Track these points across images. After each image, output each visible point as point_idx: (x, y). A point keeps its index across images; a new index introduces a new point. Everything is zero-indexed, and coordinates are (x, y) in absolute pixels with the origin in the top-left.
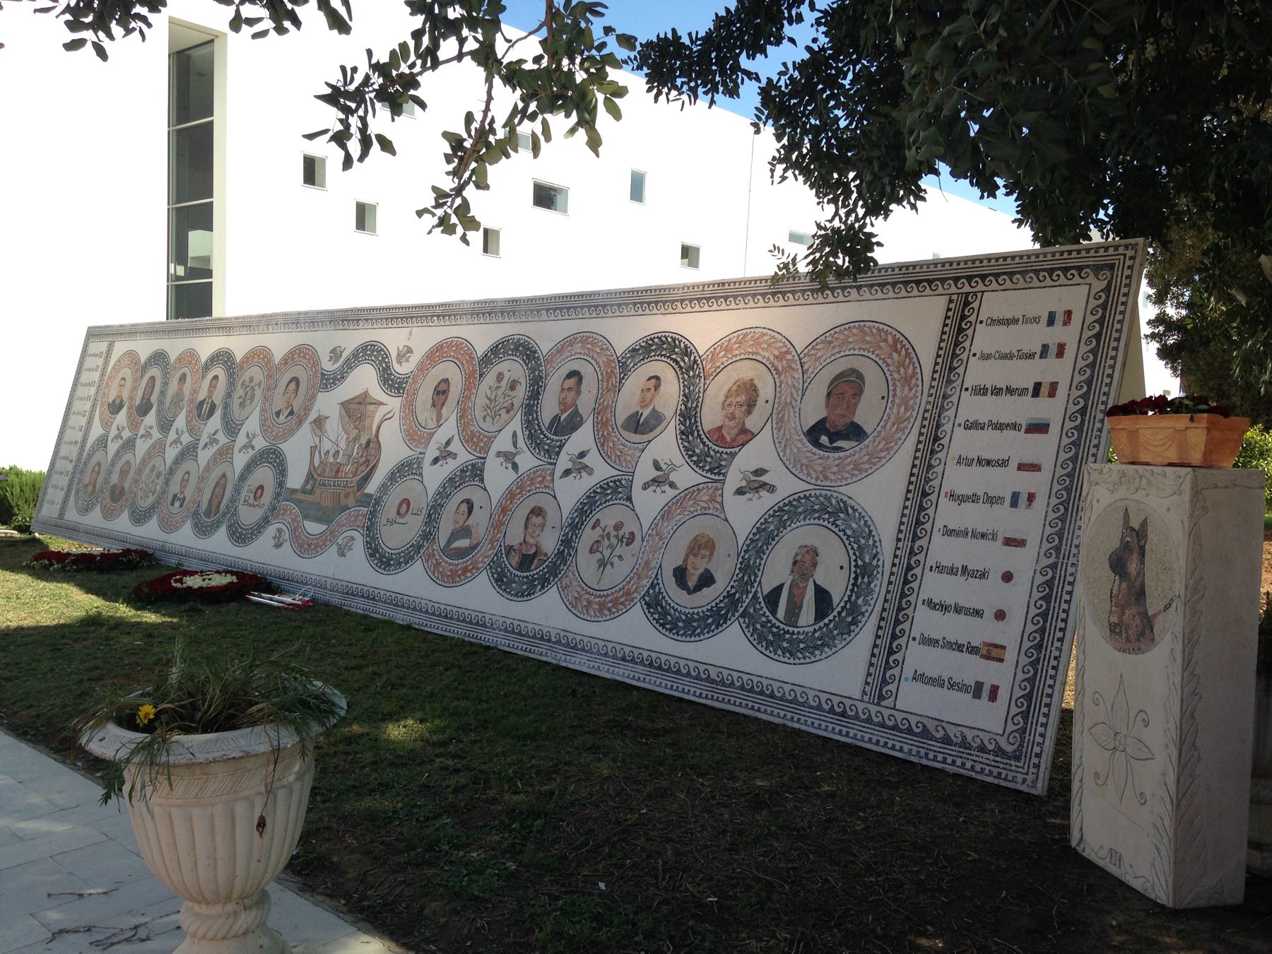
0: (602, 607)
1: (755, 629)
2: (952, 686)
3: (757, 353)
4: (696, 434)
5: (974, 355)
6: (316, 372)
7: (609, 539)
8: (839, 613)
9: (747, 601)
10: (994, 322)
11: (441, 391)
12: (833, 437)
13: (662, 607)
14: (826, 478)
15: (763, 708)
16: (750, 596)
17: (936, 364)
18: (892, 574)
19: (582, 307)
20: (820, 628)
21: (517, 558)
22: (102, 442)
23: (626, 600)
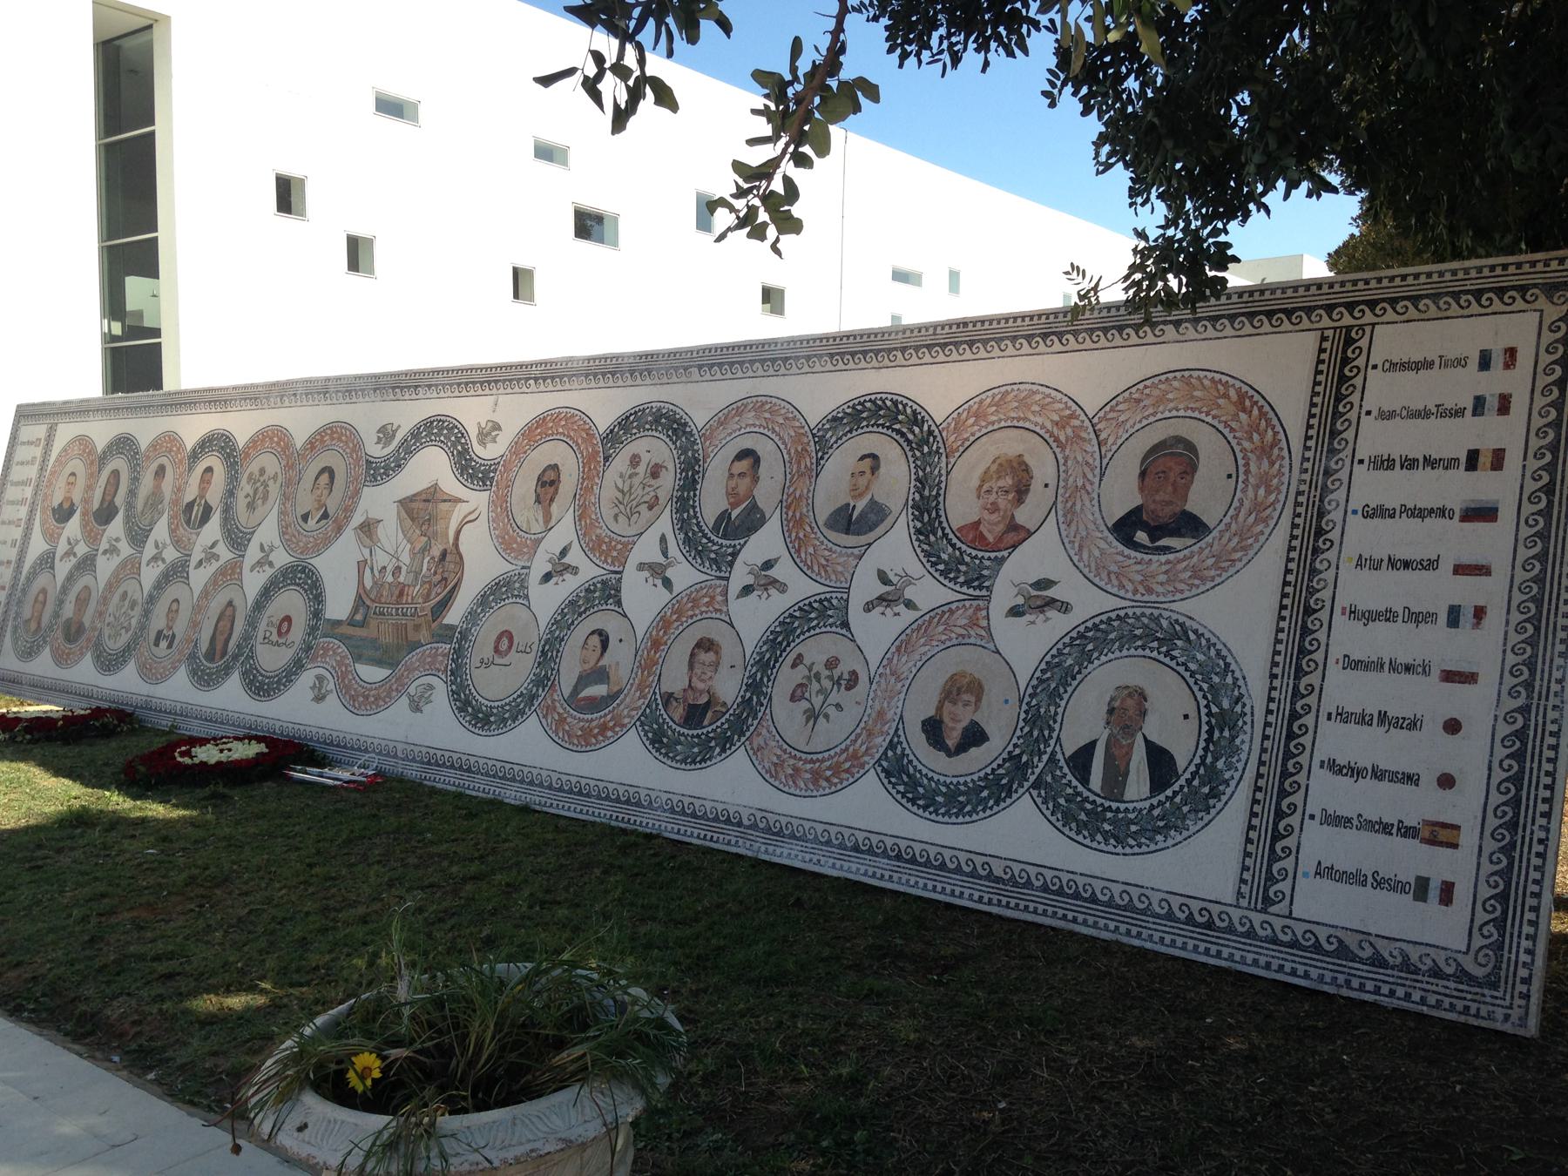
0: (817, 776)
1: (1057, 806)
2: (1379, 883)
3: (1026, 419)
4: (940, 533)
5: (1369, 413)
6: (358, 460)
7: (819, 681)
8: (1189, 782)
9: (1041, 765)
10: (1393, 366)
11: (548, 482)
12: (1156, 532)
13: (909, 776)
14: (1150, 591)
15: (1081, 918)
16: (1045, 758)
17: (1309, 427)
18: (1267, 724)
19: (752, 362)
20: (1160, 803)
21: (681, 710)
22: (47, 561)
23: (853, 766)
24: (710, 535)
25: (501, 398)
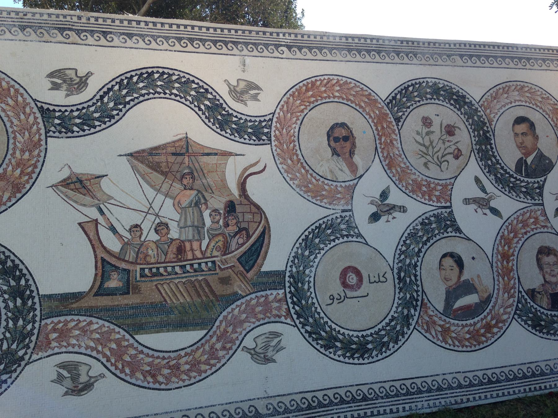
6: (18, 108)
24: (515, 175)
25: (248, 60)
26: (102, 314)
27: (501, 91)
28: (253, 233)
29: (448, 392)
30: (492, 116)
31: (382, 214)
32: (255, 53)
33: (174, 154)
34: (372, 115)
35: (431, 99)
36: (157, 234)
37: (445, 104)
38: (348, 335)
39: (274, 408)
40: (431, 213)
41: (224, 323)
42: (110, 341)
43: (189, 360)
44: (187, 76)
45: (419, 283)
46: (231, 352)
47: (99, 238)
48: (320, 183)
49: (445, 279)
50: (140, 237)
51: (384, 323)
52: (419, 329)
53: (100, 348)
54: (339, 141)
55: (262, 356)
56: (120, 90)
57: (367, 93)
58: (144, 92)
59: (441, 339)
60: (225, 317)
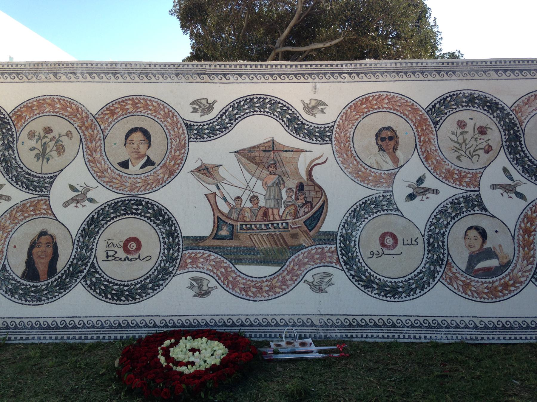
6: (175, 124)
25: (318, 85)
26: (217, 250)
27: (533, 97)
28: (316, 205)
29: (465, 330)
30: (523, 118)
31: (418, 195)
32: (324, 80)
33: (264, 151)
34: (414, 120)
35: (466, 106)
36: (251, 203)
37: (479, 110)
38: (383, 280)
39: (325, 322)
40: (461, 195)
41: (292, 264)
42: (221, 267)
43: (269, 284)
44: (276, 99)
45: (445, 247)
46: (296, 283)
47: (216, 204)
48: (368, 171)
49: (469, 246)
50: (241, 204)
51: (413, 275)
52: (443, 281)
53: (215, 271)
54: (385, 140)
55: (318, 287)
56: (233, 111)
57: (410, 104)
58: (247, 111)
59: (462, 291)
60: (293, 260)
